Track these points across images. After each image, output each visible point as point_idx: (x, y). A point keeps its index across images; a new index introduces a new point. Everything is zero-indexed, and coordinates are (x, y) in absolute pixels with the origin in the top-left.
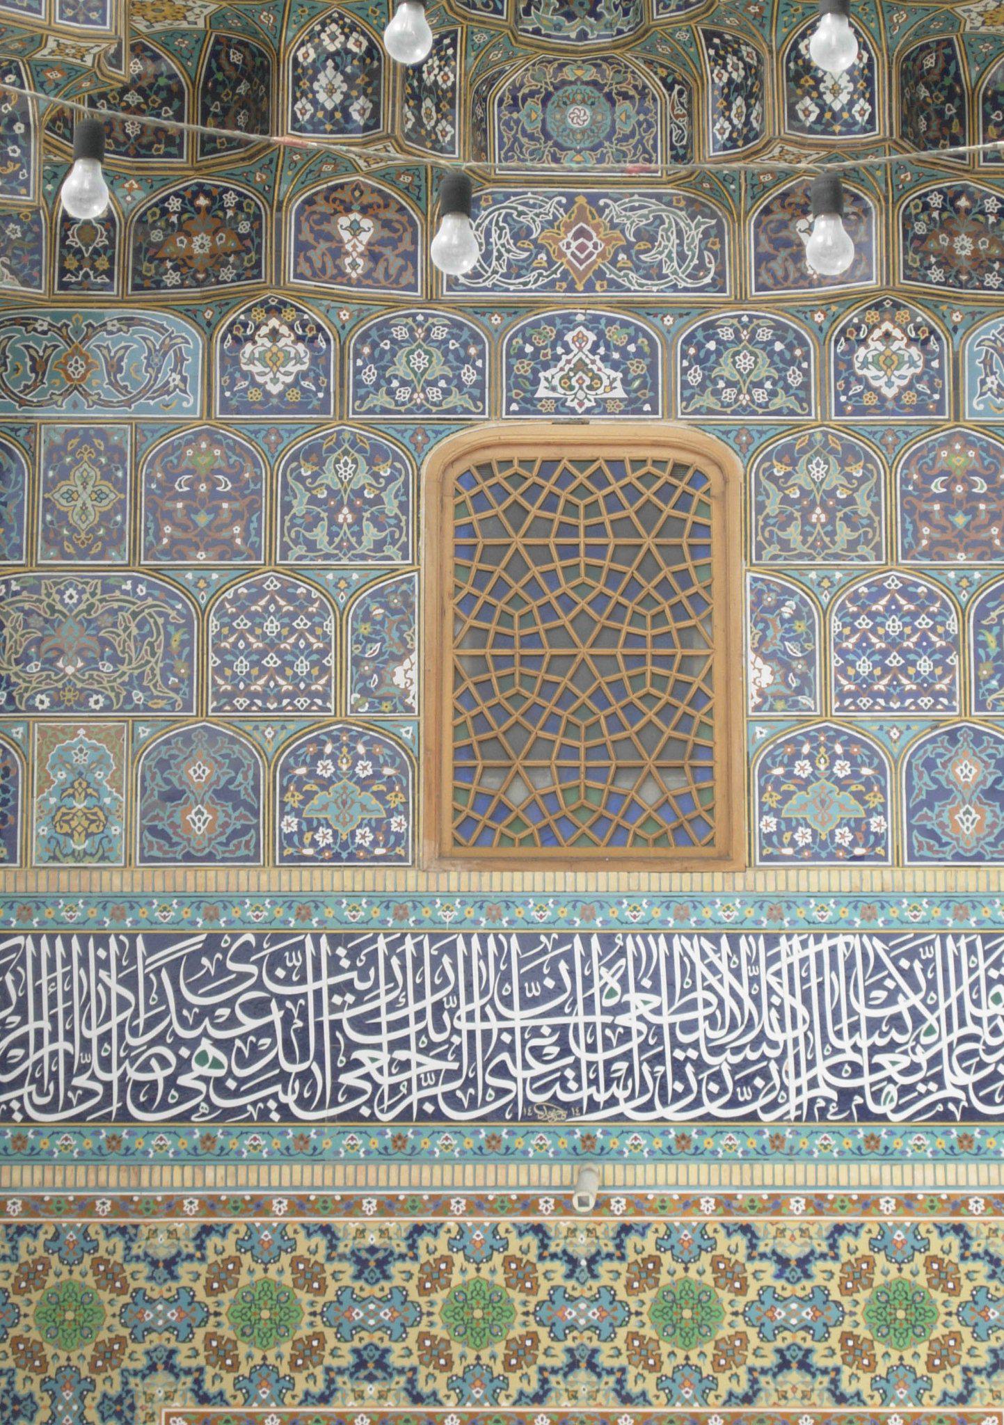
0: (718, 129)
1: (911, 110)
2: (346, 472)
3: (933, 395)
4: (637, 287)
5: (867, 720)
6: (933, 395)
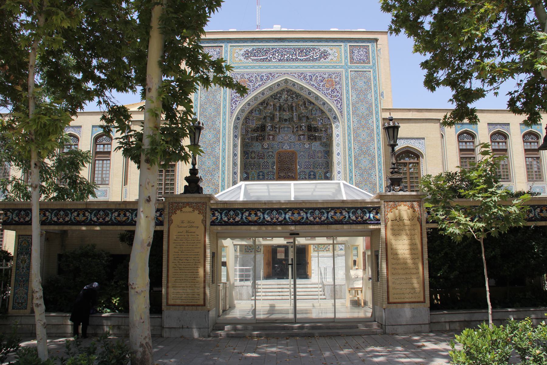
0: (295, 130)
1: (308, 129)
2: (271, 153)
3: (310, 148)
4: (290, 141)
5: (305, 170)
6: (310, 148)
